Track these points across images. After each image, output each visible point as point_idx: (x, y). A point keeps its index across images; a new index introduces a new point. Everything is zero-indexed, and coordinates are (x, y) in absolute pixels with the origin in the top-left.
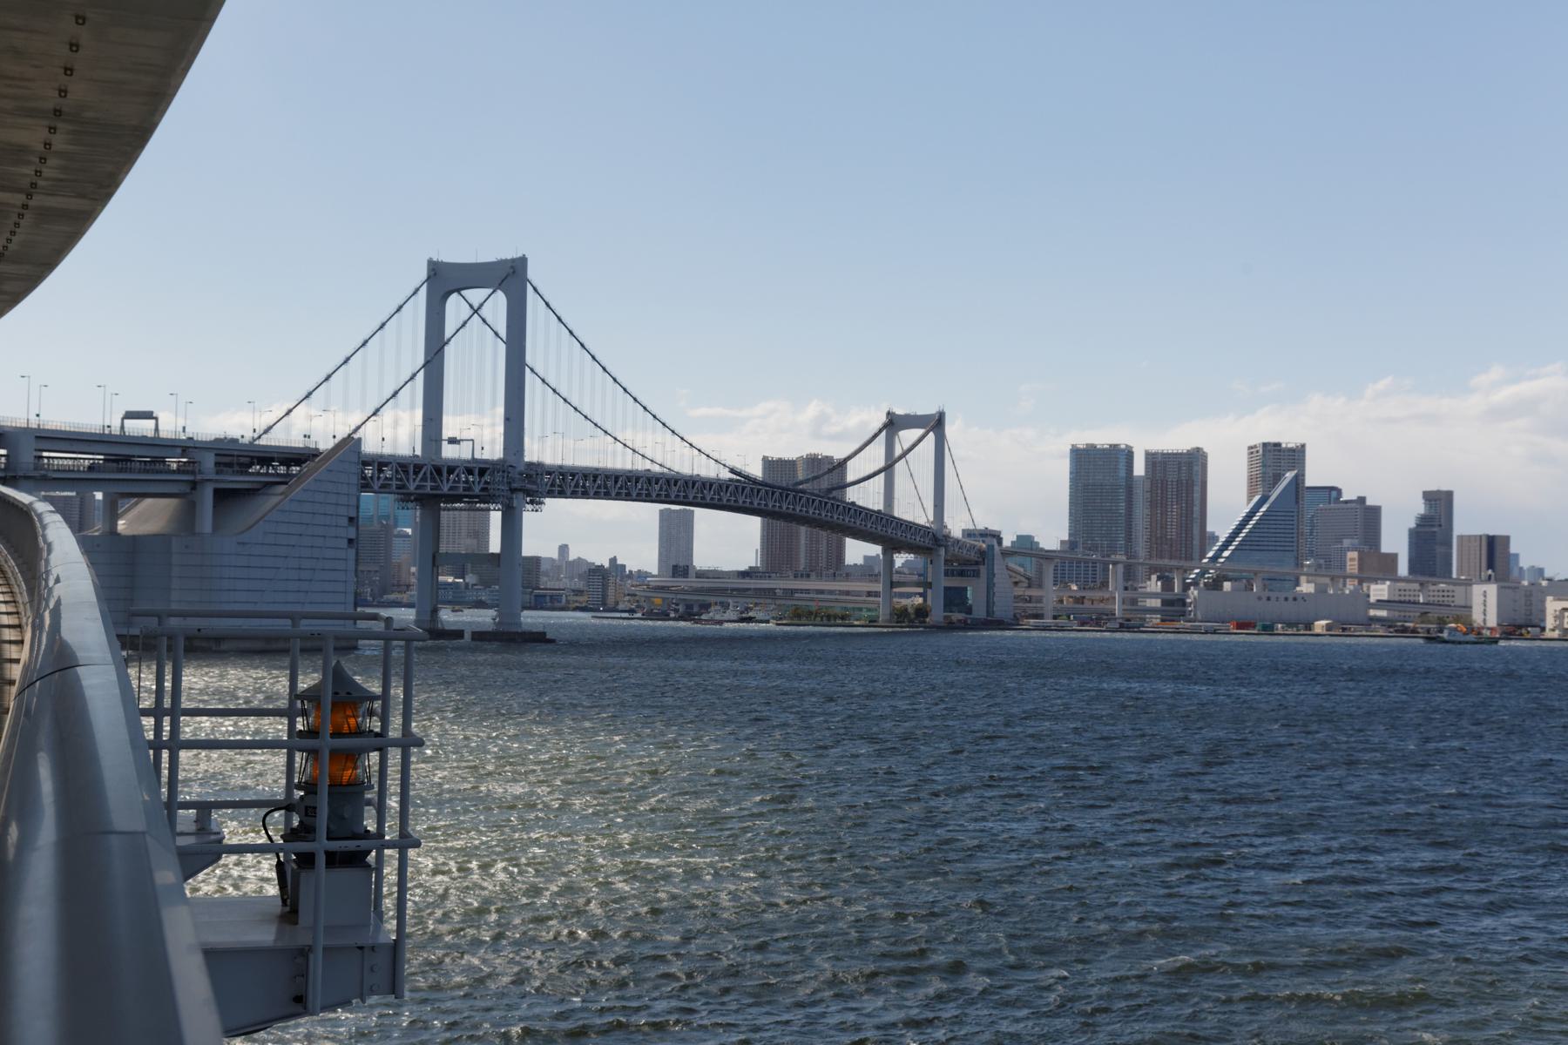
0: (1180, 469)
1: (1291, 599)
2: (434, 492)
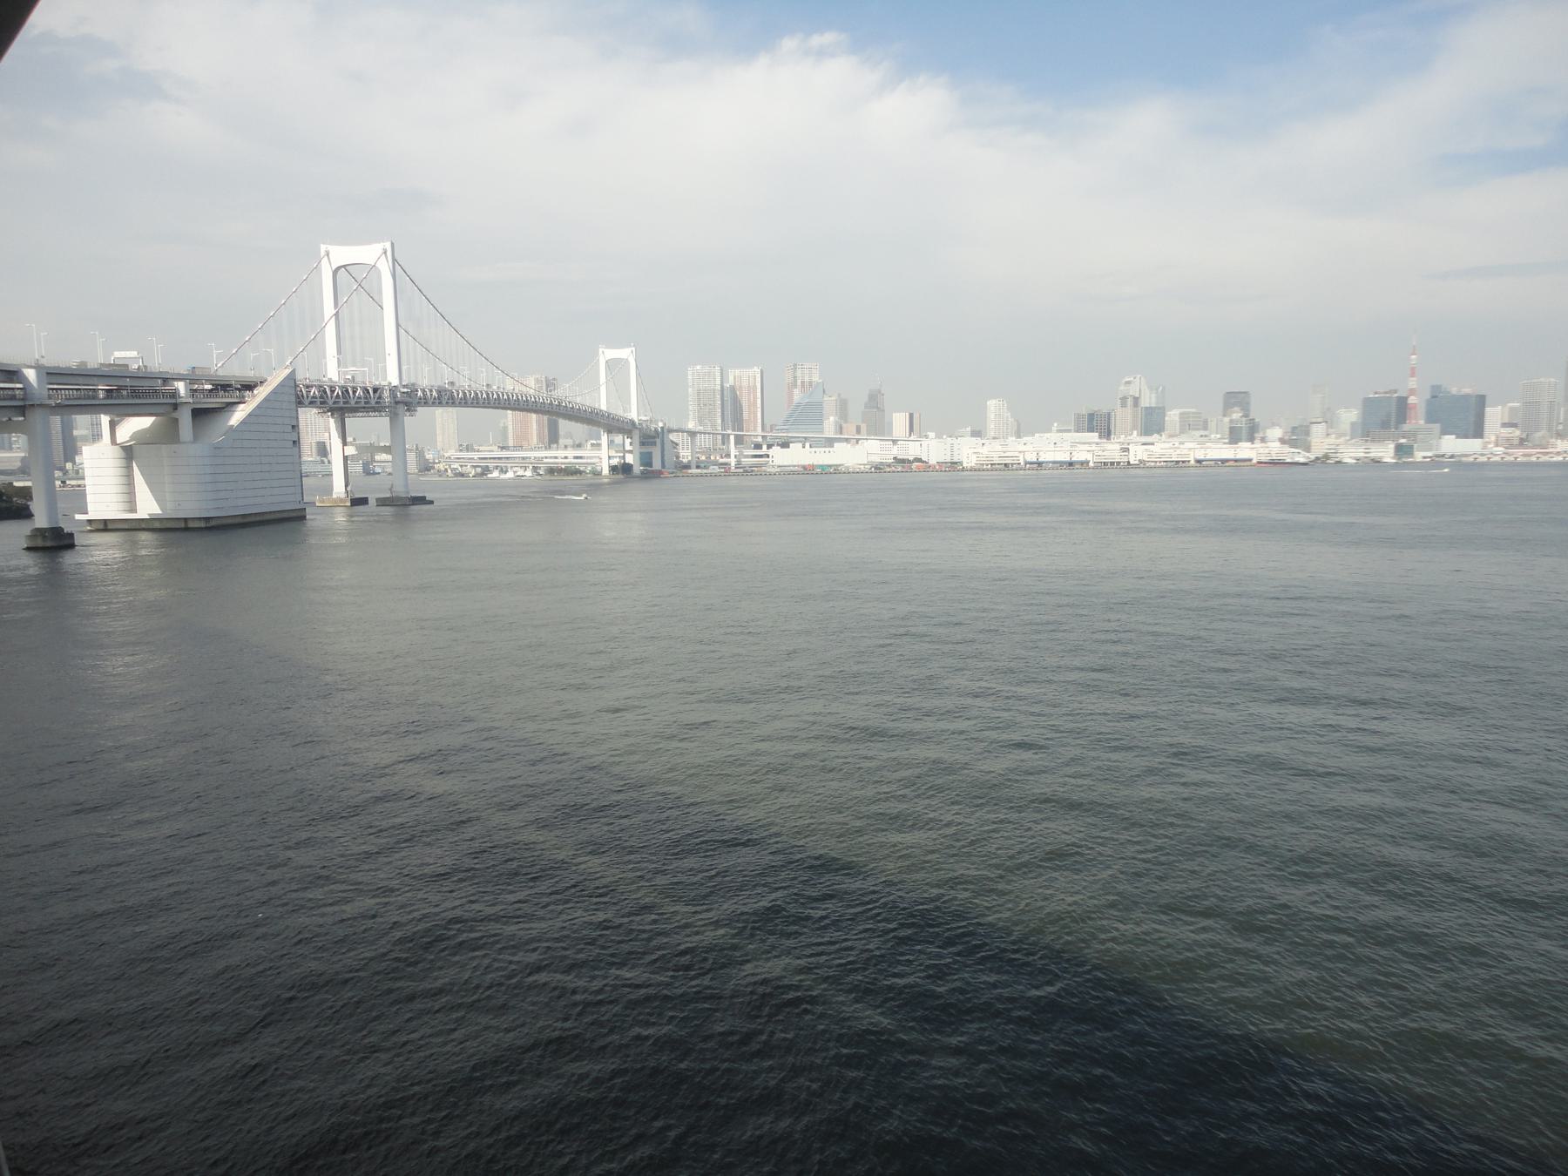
1: (827, 452)
2: (346, 406)
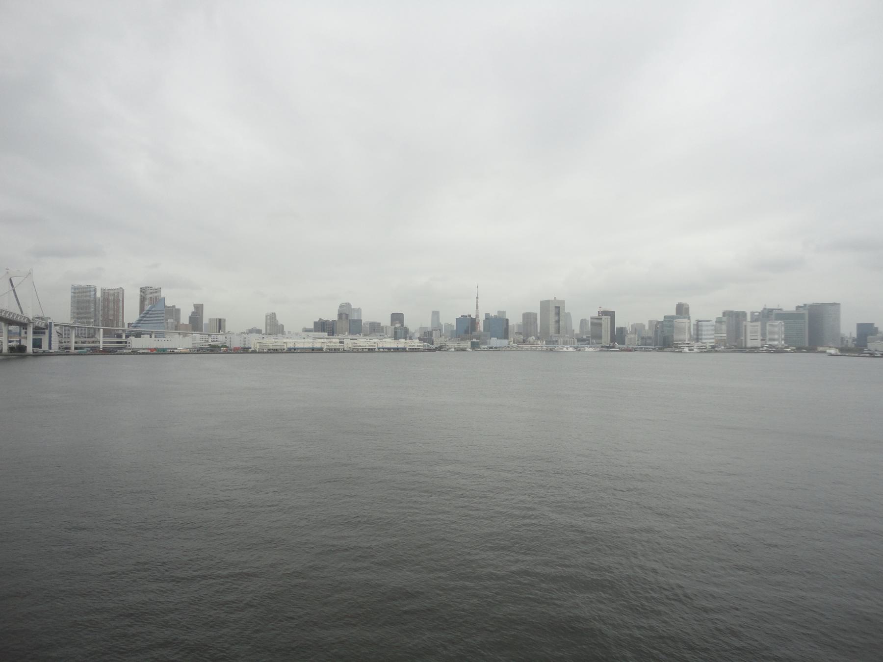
0: (114, 295)
1: (166, 340)
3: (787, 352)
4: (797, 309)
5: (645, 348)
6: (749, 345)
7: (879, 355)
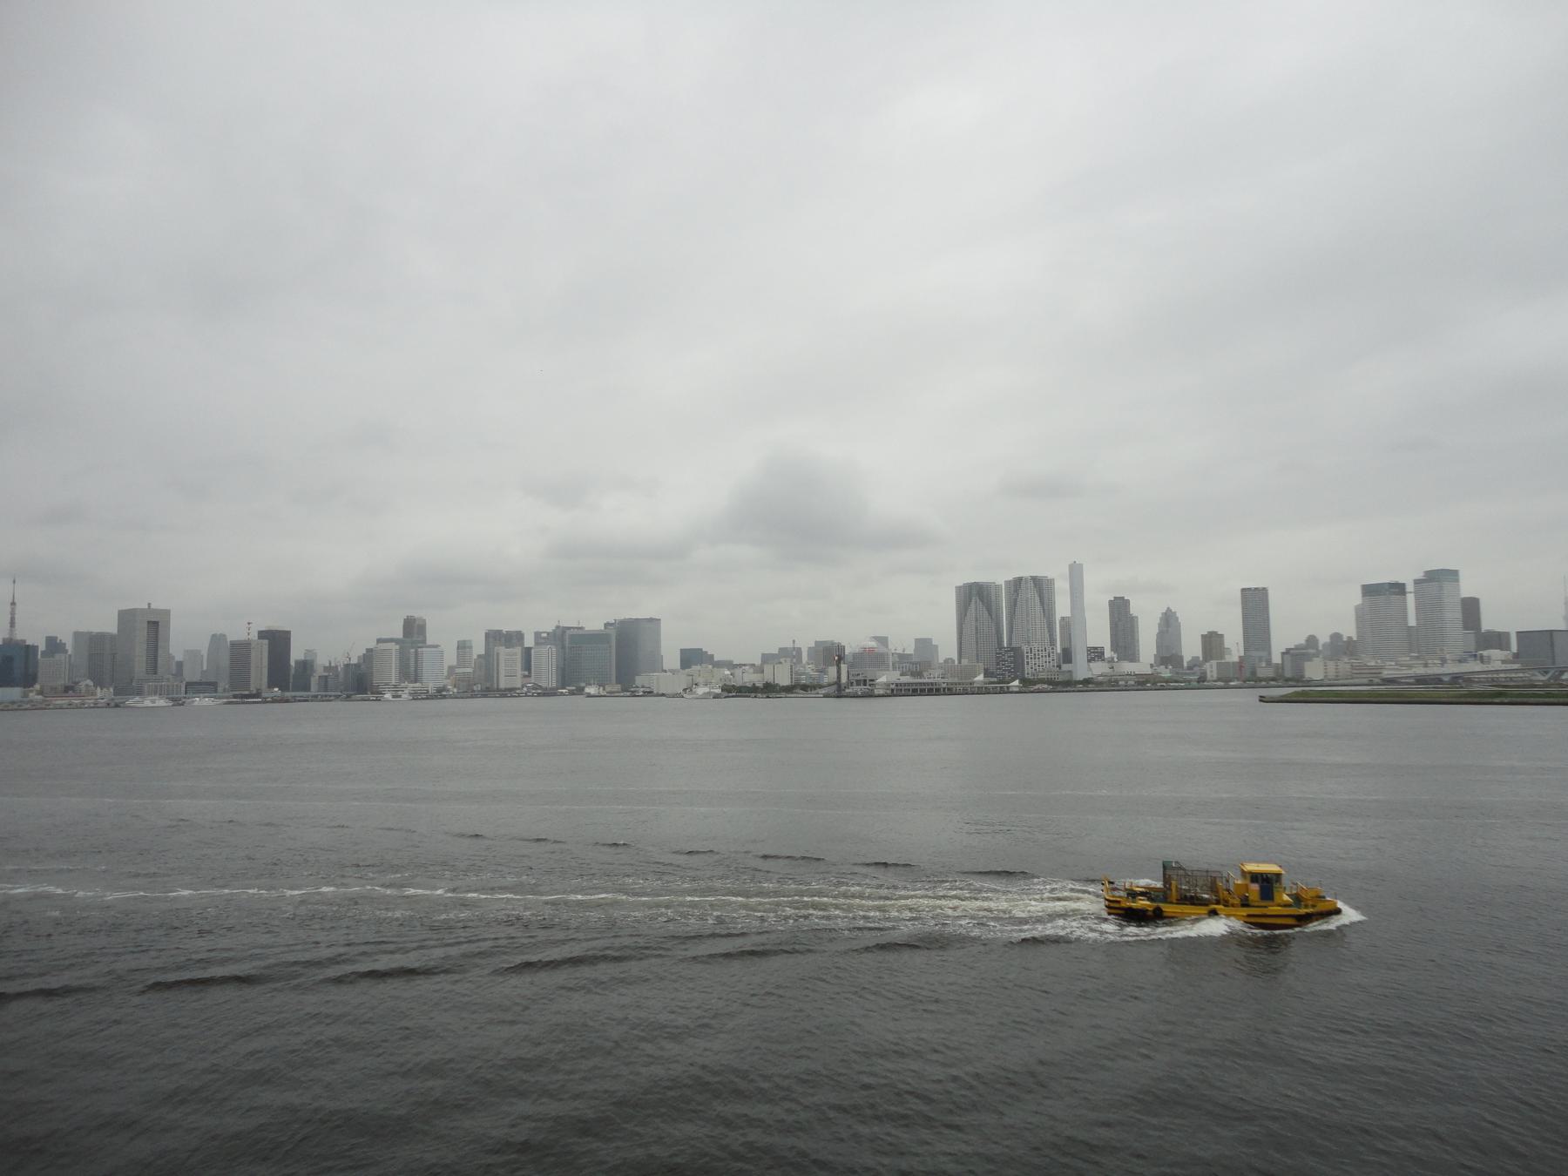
3: (562, 694)
4: (605, 628)
5: (322, 696)
6: (502, 686)
7: (641, 694)
